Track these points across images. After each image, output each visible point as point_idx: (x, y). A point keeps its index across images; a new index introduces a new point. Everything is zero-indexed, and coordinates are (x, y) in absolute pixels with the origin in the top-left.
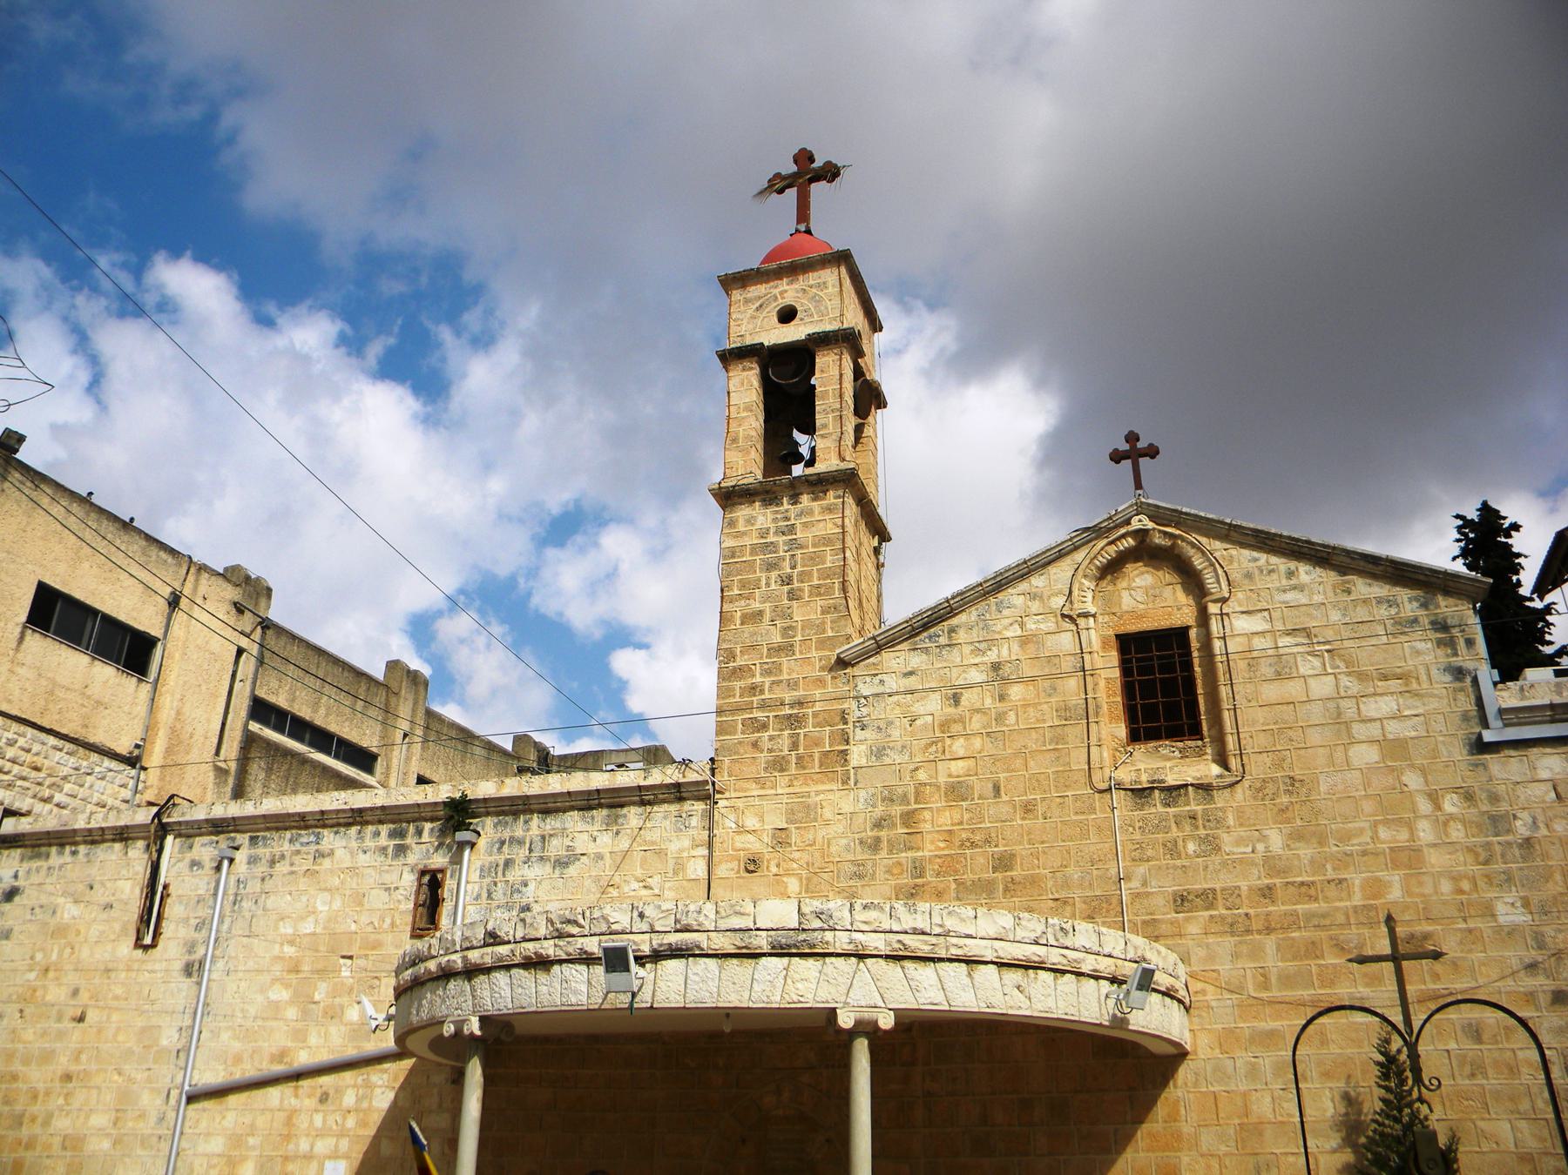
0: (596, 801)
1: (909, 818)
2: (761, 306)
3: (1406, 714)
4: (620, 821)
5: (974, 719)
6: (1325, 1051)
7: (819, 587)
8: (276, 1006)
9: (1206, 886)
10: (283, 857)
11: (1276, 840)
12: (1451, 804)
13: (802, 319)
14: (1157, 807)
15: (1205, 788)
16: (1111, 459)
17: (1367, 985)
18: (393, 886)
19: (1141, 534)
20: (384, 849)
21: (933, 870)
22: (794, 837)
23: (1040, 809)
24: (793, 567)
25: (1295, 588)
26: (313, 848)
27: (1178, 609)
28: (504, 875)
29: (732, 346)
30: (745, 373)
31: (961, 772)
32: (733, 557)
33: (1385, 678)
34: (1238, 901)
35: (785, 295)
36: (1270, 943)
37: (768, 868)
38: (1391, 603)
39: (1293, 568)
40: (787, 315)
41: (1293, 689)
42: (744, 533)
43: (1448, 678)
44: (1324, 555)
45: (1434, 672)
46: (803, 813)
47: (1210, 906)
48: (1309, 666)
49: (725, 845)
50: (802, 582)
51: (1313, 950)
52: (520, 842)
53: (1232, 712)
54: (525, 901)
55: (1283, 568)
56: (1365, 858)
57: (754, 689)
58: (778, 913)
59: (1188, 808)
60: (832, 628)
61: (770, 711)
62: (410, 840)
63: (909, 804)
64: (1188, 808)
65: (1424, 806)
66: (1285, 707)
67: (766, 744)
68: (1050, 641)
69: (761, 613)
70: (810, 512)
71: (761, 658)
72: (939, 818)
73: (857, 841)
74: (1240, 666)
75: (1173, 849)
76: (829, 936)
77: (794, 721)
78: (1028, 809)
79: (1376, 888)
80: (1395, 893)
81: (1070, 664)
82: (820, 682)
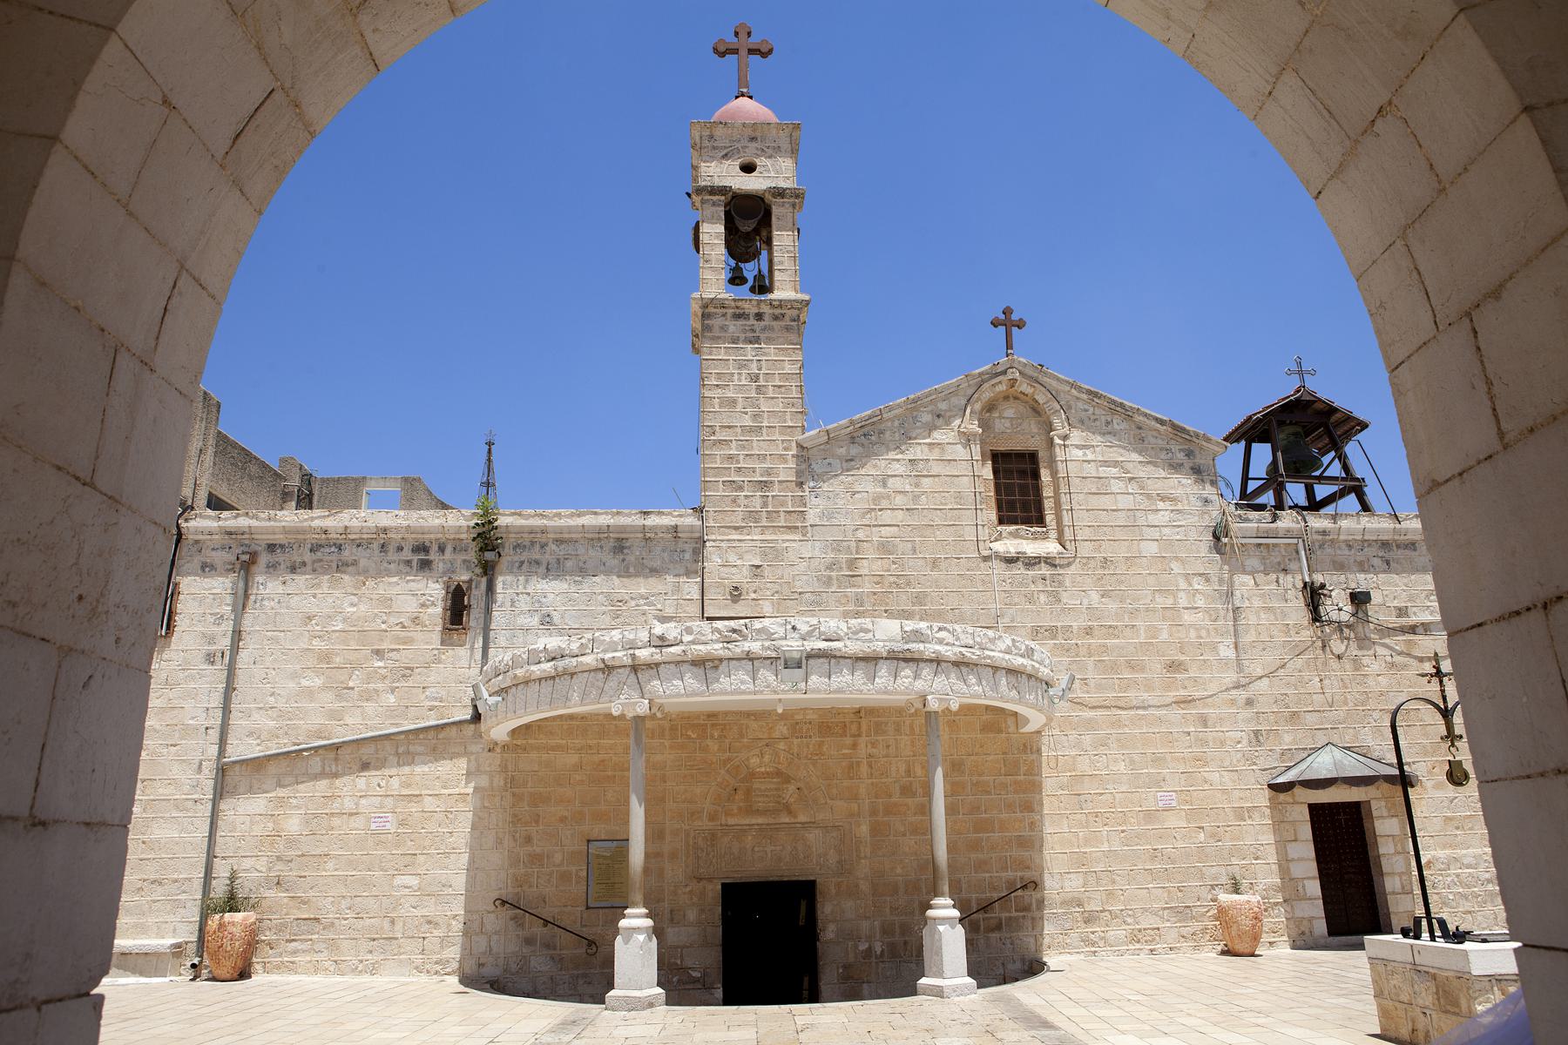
0: (606, 535)
1: (852, 564)
2: (726, 155)
3: (1175, 524)
4: (625, 551)
5: (897, 498)
6: (1122, 732)
7: (780, 387)
8: (309, 693)
9: (1052, 624)
10: (304, 564)
11: (1095, 596)
12: (1198, 584)
13: (761, 173)
14: (1019, 570)
15: (1049, 561)
16: (992, 323)
17: (1147, 691)
18: (419, 593)
19: (1013, 382)
20: (408, 563)
21: (870, 602)
22: (767, 572)
23: (943, 565)
24: (760, 369)
25: (1110, 433)
26: (334, 557)
27: (1033, 437)
28: (525, 588)
29: (704, 184)
30: (714, 209)
31: (888, 535)
32: (710, 354)
33: (1163, 499)
34: (1071, 635)
35: (747, 150)
36: (1090, 662)
37: (747, 593)
38: (1168, 451)
39: (1109, 420)
40: (748, 168)
41: (1106, 502)
42: (719, 338)
43: (1199, 504)
44: (1131, 414)
45: (1191, 498)
46: (774, 554)
47: (1054, 638)
48: (1116, 486)
49: (713, 575)
50: (767, 382)
51: (1114, 667)
52: (538, 563)
53: (1070, 512)
54: (545, 610)
55: (1103, 418)
56: (1148, 613)
57: (730, 458)
58: (887, 632)
59: (1040, 572)
60: (791, 420)
61: (745, 477)
63: (852, 554)
64: (1040, 572)
65: (1183, 585)
66: (1101, 512)
67: (742, 501)
68: (949, 448)
69: (734, 402)
70: (771, 329)
71: (736, 436)
73: (815, 579)
74: (1075, 482)
76: (921, 646)
78: (935, 563)
79: (1153, 631)
80: (1164, 636)
81: (965, 467)
82: (782, 458)
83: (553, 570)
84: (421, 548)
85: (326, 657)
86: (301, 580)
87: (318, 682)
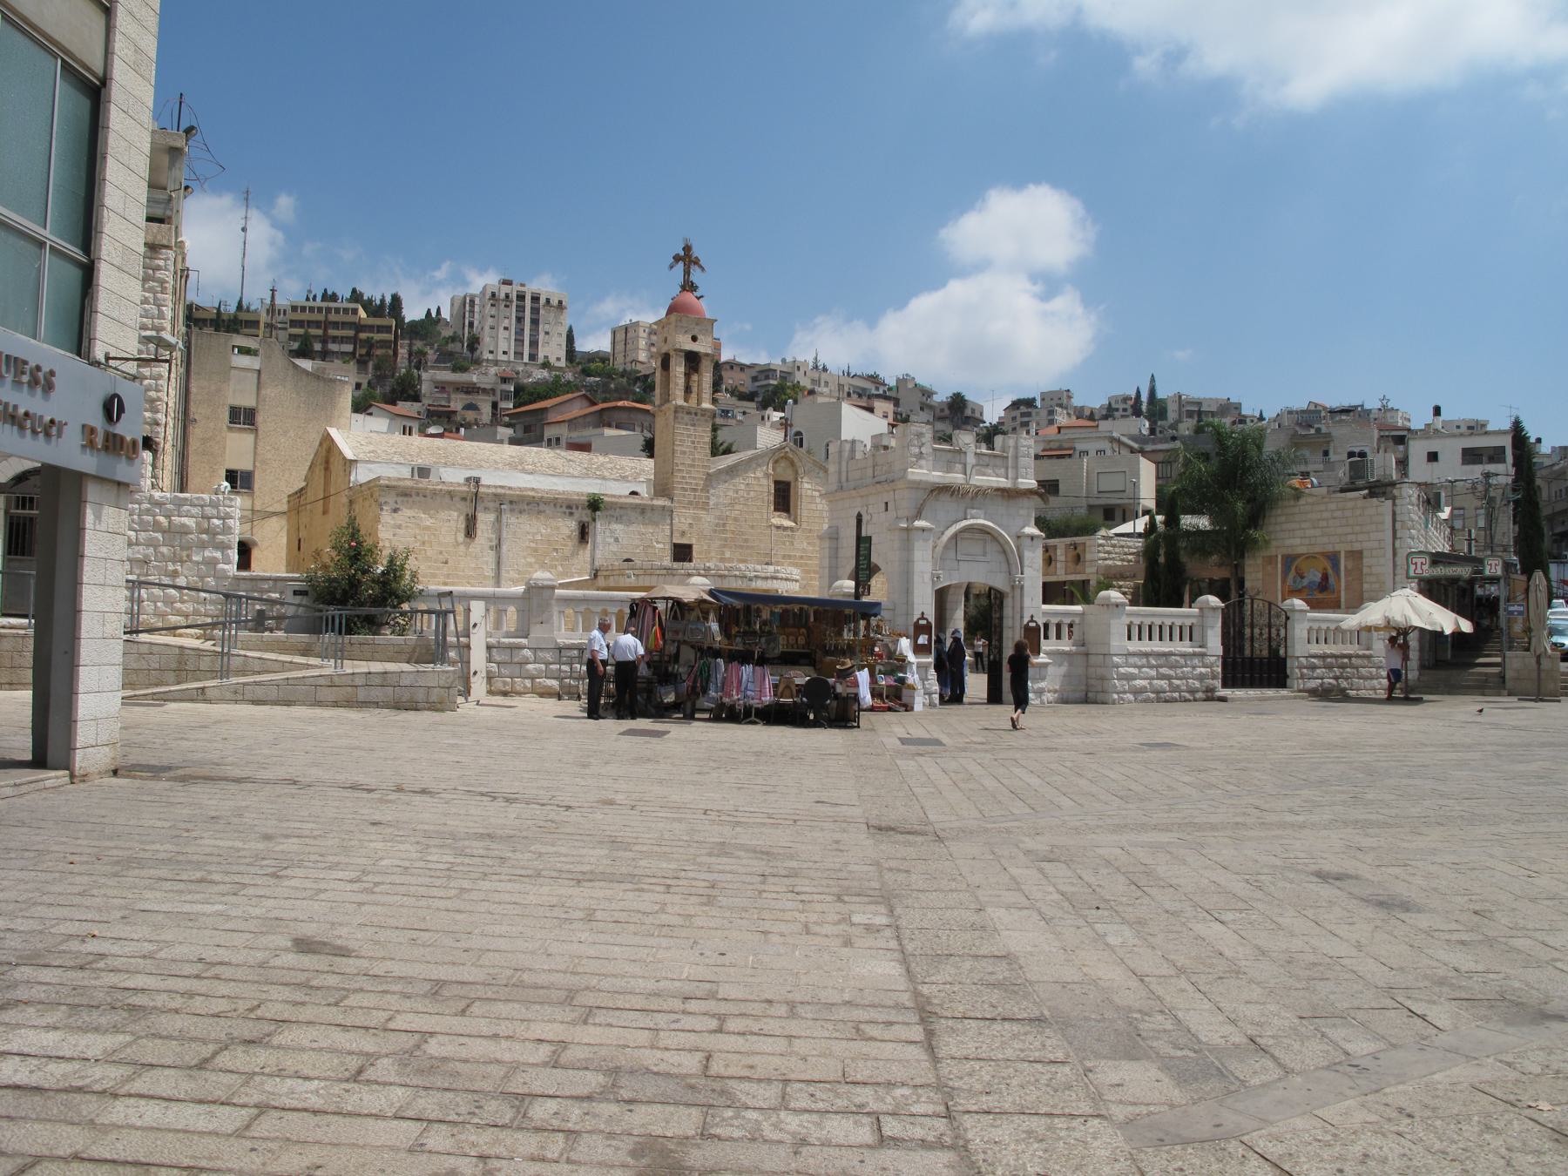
1: (724, 525)
14: (780, 532)
15: (791, 529)
41: (813, 506)
46: (697, 519)
57: (683, 477)
62: (574, 510)
72: (731, 526)
75: (784, 543)
77: (695, 490)
78: (752, 527)
83: (619, 520)
84: (569, 507)
85: (536, 550)
86: (524, 518)
87: (533, 560)
